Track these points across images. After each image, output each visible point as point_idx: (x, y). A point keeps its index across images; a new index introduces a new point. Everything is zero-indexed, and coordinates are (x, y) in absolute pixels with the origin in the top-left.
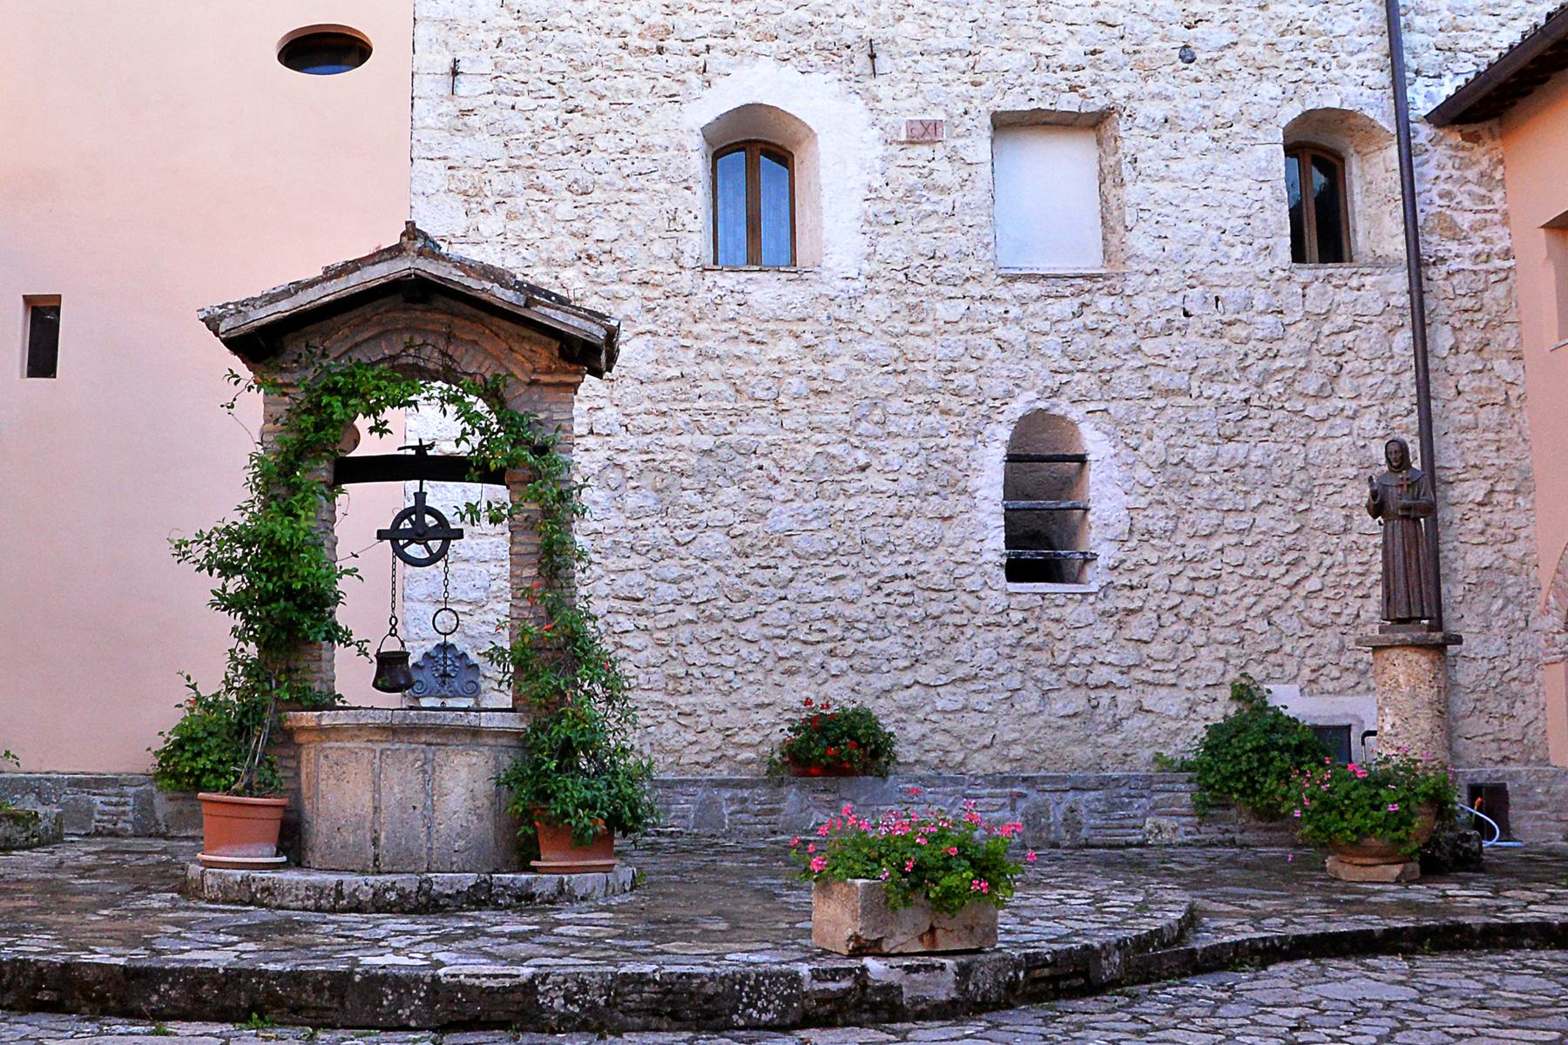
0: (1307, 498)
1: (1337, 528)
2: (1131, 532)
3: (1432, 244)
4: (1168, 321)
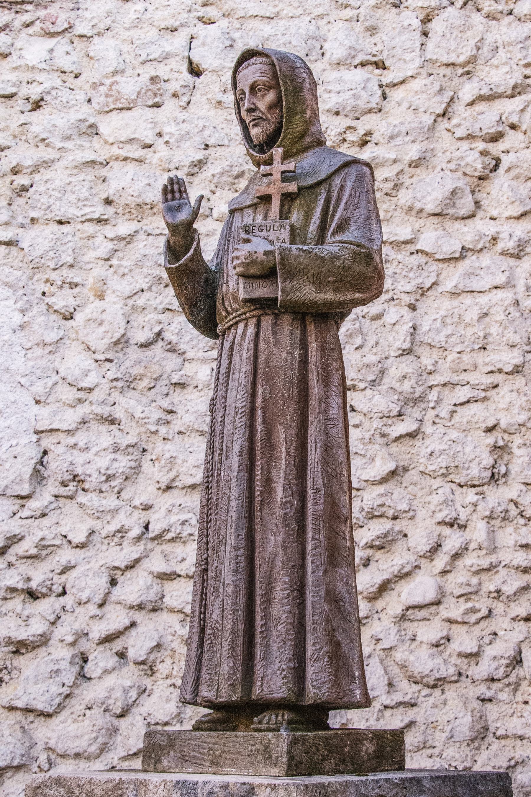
0: (416, 413)
1: (475, 471)
2: (38, 475)
4: (154, 79)
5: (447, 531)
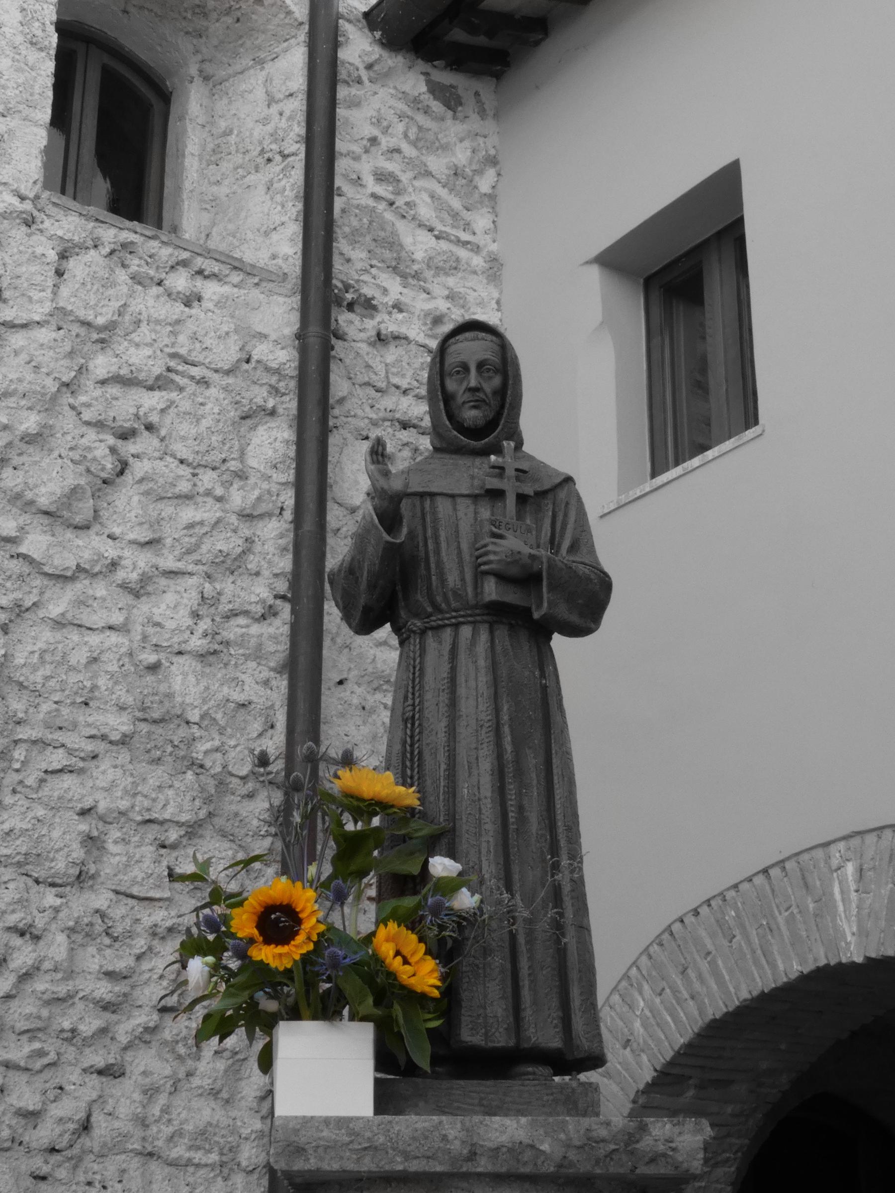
1: (60, 865)
3: (352, 261)
5: (17, 941)
